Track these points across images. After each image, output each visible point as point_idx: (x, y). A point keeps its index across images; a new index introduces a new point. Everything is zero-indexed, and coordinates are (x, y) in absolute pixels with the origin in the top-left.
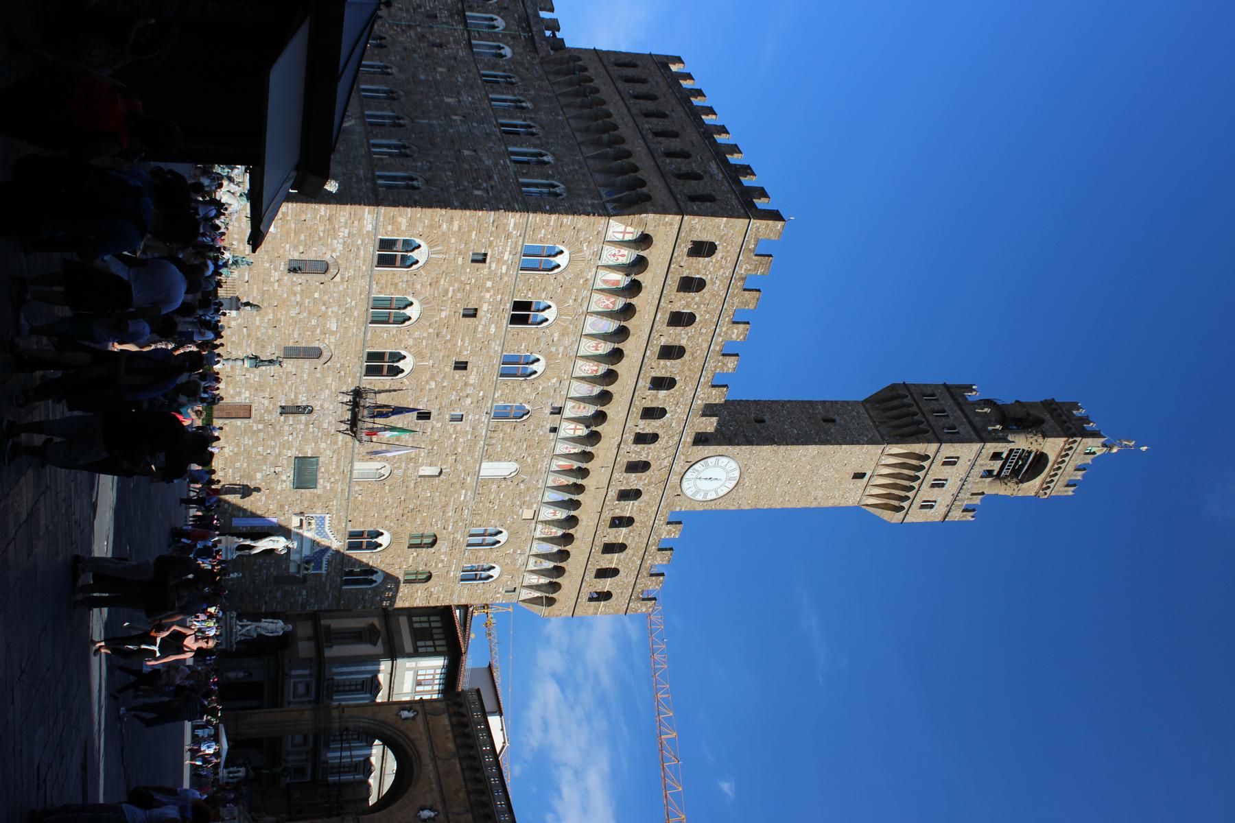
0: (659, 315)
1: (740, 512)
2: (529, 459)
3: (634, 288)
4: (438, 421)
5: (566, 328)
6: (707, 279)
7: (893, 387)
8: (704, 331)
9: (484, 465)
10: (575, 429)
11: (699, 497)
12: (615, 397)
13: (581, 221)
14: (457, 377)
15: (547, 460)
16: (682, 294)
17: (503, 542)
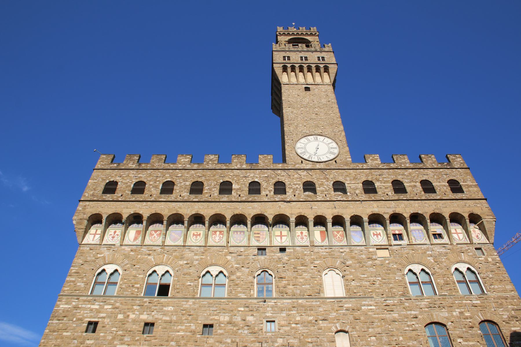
0: (160, 200)
1: (345, 130)
2: (316, 262)
3: (136, 219)
4: (276, 342)
5: (176, 257)
6: (135, 181)
7: (273, 112)
8: (180, 175)
9: (326, 296)
10: (281, 236)
11: (336, 151)
12: (237, 212)
13: (78, 261)
14: (220, 331)
15: (316, 250)
16: (145, 191)
17: (422, 267)
